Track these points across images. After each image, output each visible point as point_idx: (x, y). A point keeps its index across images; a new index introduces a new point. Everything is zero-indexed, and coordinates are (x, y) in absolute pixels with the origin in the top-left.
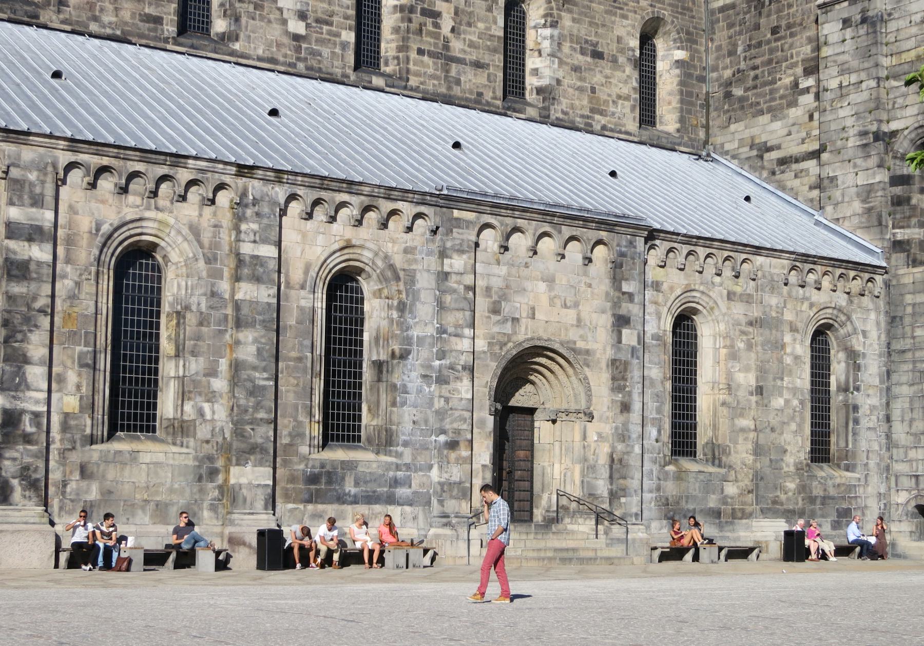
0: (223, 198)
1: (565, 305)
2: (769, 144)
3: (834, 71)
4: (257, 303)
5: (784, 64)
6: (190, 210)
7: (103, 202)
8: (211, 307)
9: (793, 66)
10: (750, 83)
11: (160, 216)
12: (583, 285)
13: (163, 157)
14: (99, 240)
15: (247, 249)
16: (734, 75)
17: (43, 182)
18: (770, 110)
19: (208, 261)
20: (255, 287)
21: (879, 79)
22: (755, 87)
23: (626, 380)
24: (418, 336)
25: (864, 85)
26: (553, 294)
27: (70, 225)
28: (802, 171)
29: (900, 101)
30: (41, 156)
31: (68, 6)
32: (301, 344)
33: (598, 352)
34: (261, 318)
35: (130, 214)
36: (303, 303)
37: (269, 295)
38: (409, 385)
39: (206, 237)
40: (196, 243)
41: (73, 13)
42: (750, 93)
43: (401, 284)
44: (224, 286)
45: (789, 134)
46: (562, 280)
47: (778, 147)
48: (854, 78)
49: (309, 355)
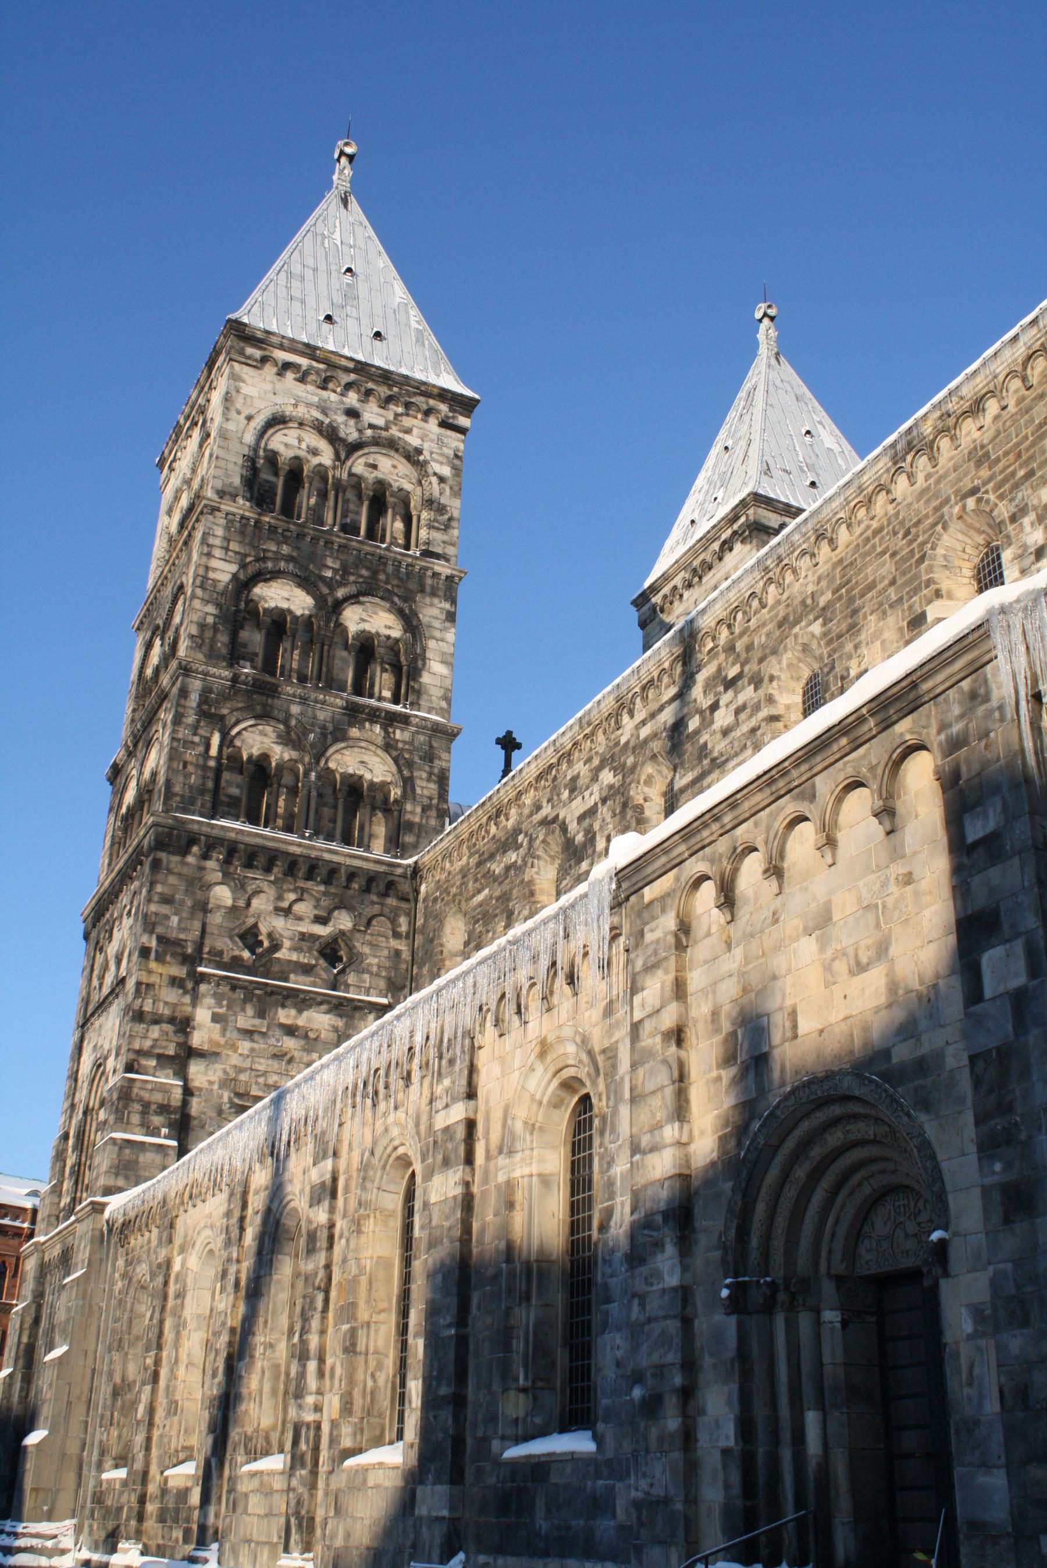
1: (858, 963)
12: (893, 888)
23: (1010, 1109)
24: (622, 1174)
26: (829, 954)
33: (950, 1051)
38: (613, 1282)
43: (601, 1080)
46: (844, 906)
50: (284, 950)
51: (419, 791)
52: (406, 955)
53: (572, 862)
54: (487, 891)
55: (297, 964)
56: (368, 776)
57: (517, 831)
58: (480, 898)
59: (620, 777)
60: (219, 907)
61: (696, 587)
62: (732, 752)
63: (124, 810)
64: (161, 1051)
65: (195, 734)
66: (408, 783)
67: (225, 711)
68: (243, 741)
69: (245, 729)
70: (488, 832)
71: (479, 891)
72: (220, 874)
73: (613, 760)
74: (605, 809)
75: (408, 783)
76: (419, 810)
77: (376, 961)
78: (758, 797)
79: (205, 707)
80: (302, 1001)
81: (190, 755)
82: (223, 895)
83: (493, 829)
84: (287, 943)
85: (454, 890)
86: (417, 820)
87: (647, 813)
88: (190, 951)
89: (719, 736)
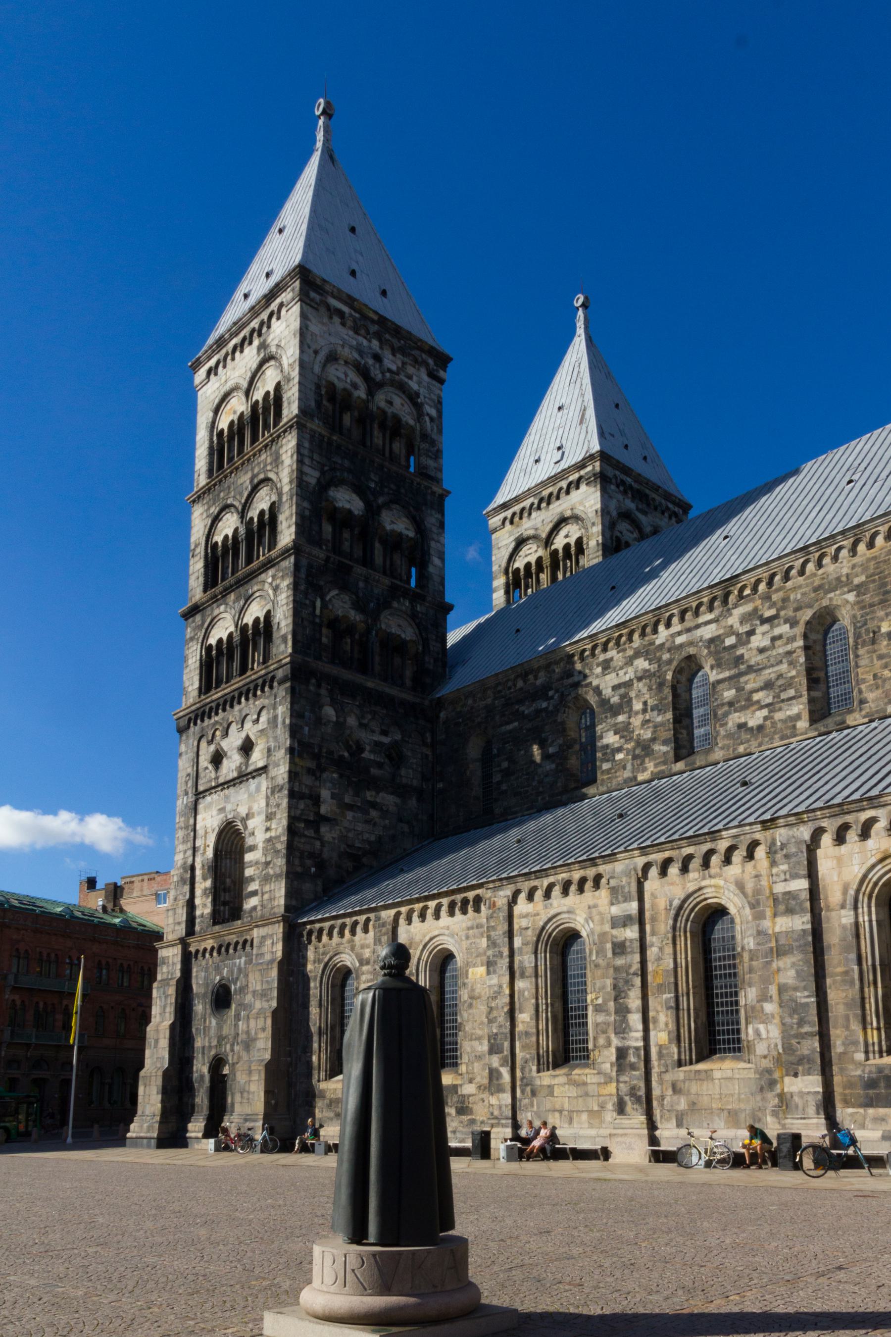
0: (760, 852)
4: (793, 931)
6: (735, 870)
7: (672, 884)
8: (758, 944)
11: (713, 882)
13: (703, 838)
14: (673, 912)
15: (780, 888)
17: (629, 884)
19: (753, 906)
20: (790, 919)
27: (653, 906)
30: (627, 866)
31: (868, 702)
32: (847, 959)
34: (797, 944)
35: (691, 887)
36: (844, 921)
37: (803, 923)
39: (749, 886)
40: (741, 895)
41: (872, 705)
44: (766, 924)
49: (856, 968)
50: (366, 752)
51: (432, 648)
52: (430, 758)
53: (609, 715)
54: (516, 724)
55: (374, 761)
56: (403, 636)
57: (546, 688)
58: (510, 727)
59: (656, 666)
60: (329, 721)
61: (543, 511)
62: (768, 664)
63: (213, 641)
64: (306, 817)
65: (306, 598)
66: (425, 642)
67: (322, 583)
68: (333, 605)
69: (333, 597)
70: (515, 685)
71: (508, 723)
72: (329, 699)
73: (647, 654)
74: (641, 684)
75: (425, 642)
76: (432, 661)
77: (415, 761)
79: (310, 579)
80: (374, 784)
81: (305, 613)
82: (329, 712)
83: (520, 684)
84: (368, 748)
85: (479, 719)
86: (431, 667)
87: (679, 691)
88: (316, 751)
89: (755, 652)
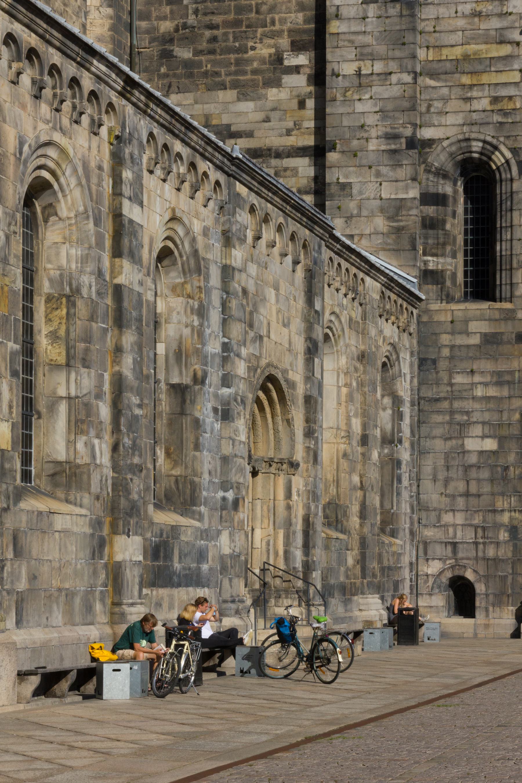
2: (233, 129)
3: (351, 54)
5: (260, 30)
9: (278, 34)
10: (204, 45)
16: (177, 30)
18: (235, 85)
21: (416, 75)
22: (212, 52)
25: (394, 78)
28: (286, 169)
29: (438, 105)
42: (203, 58)
45: (267, 120)
47: (250, 134)
48: (379, 67)
78: (278, 200)
